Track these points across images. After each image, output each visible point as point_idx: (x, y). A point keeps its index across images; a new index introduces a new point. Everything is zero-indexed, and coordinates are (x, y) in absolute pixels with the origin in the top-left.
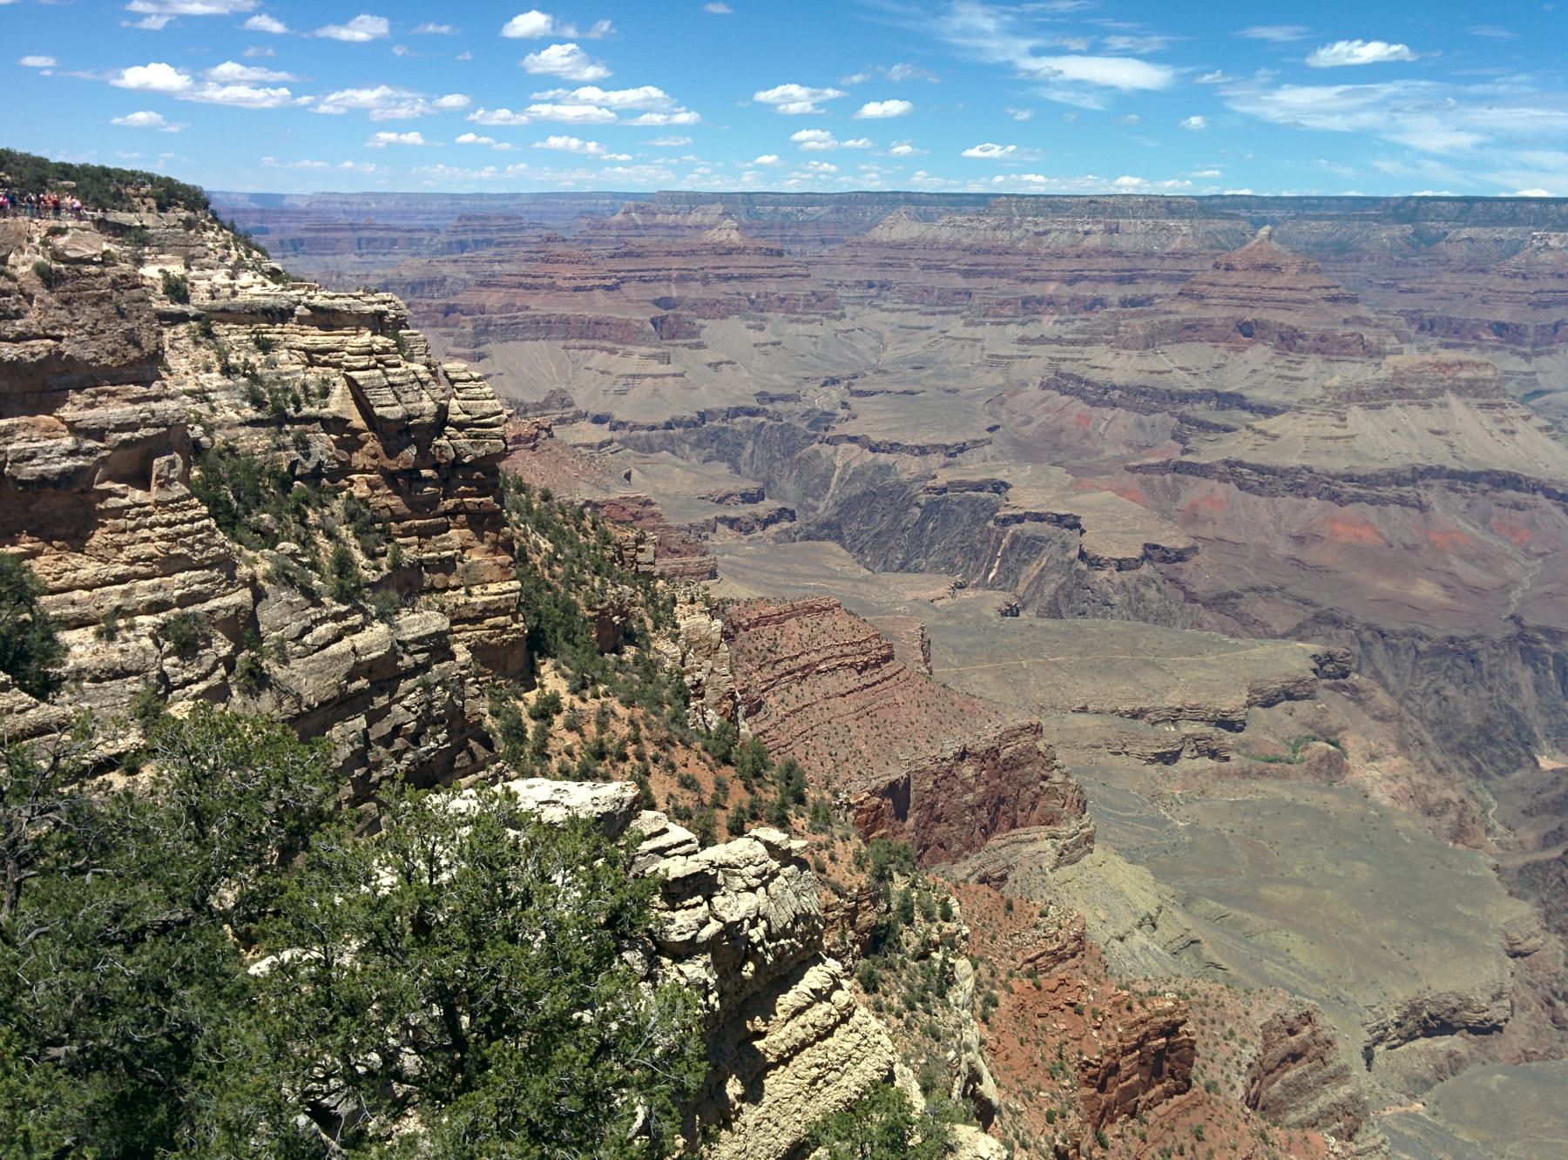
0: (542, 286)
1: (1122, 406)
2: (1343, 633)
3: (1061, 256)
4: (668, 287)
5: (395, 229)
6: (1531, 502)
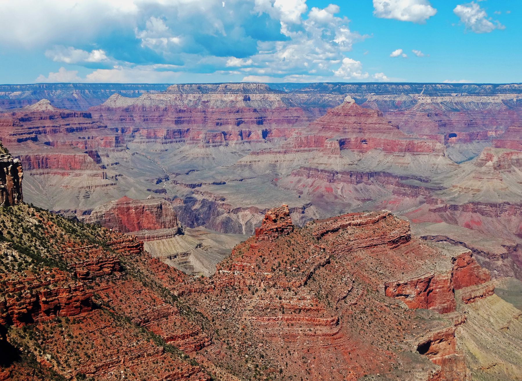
1: (344, 181)
4: (46, 137)
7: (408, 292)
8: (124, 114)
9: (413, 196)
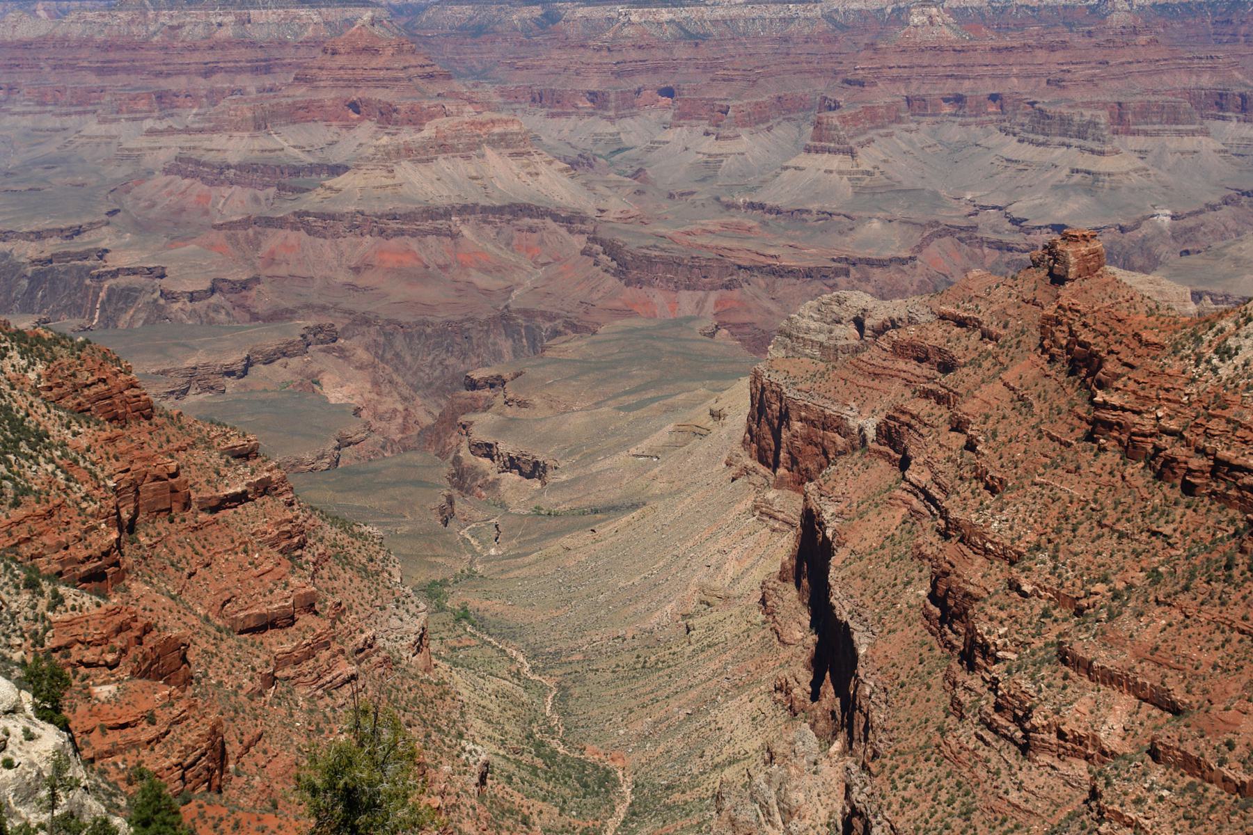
1: (238, 183)
2: (372, 330)
3: (193, 48)
6: (541, 225)
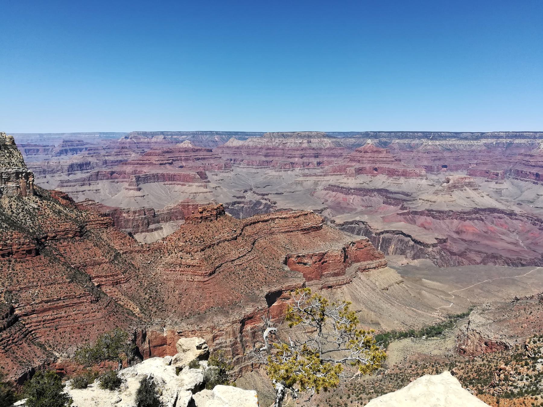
0: (147, 164)
1: (355, 194)
4: (181, 163)
5: (38, 146)
7: (306, 261)
8: (236, 150)
9: (396, 205)
